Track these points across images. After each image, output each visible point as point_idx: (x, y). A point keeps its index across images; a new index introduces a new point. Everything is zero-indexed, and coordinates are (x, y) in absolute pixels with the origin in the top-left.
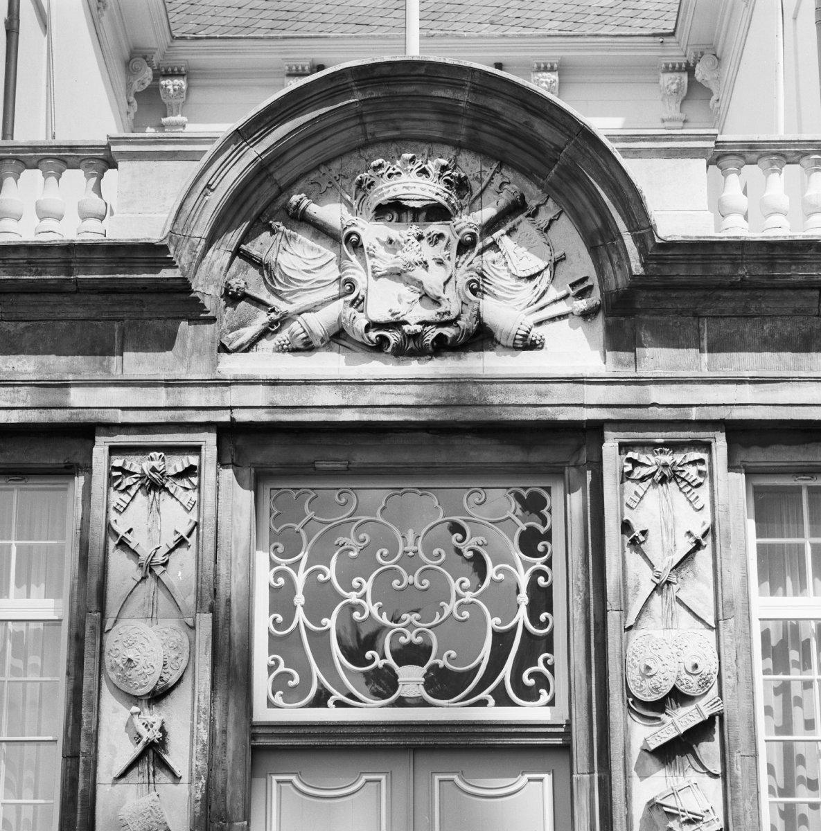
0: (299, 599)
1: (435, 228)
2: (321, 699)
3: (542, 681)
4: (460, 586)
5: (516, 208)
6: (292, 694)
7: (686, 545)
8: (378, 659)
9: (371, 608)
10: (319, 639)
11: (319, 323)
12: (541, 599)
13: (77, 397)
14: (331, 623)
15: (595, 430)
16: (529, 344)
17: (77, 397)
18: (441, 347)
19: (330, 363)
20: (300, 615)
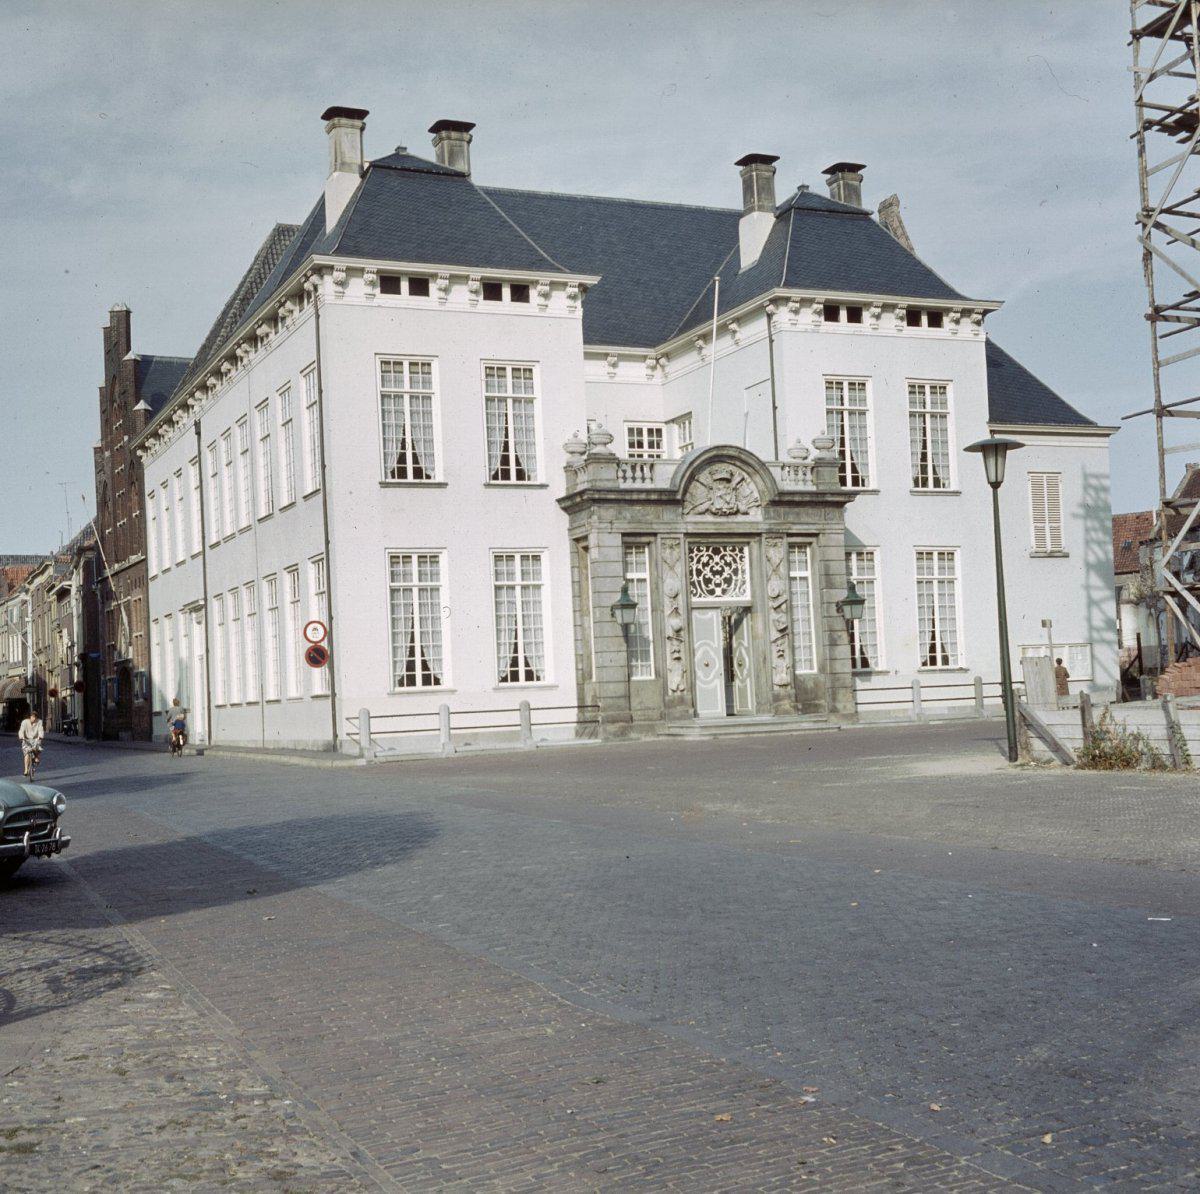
0: (694, 573)
1: (727, 485)
2: (700, 596)
3: (744, 591)
4: (727, 569)
5: (743, 479)
6: (695, 595)
7: (778, 561)
8: (712, 586)
9: (709, 575)
10: (699, 582)
11: (702, 508)
12: (743, 572)
13: (655, 526)
14: (701, 578)
15: (759, 535)
16: (746, 513)
17: (655, 526)
18: (730, 514)
19: (709, 518)
20: (695, 577)
